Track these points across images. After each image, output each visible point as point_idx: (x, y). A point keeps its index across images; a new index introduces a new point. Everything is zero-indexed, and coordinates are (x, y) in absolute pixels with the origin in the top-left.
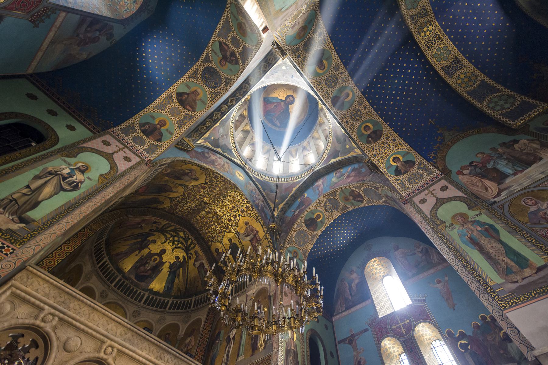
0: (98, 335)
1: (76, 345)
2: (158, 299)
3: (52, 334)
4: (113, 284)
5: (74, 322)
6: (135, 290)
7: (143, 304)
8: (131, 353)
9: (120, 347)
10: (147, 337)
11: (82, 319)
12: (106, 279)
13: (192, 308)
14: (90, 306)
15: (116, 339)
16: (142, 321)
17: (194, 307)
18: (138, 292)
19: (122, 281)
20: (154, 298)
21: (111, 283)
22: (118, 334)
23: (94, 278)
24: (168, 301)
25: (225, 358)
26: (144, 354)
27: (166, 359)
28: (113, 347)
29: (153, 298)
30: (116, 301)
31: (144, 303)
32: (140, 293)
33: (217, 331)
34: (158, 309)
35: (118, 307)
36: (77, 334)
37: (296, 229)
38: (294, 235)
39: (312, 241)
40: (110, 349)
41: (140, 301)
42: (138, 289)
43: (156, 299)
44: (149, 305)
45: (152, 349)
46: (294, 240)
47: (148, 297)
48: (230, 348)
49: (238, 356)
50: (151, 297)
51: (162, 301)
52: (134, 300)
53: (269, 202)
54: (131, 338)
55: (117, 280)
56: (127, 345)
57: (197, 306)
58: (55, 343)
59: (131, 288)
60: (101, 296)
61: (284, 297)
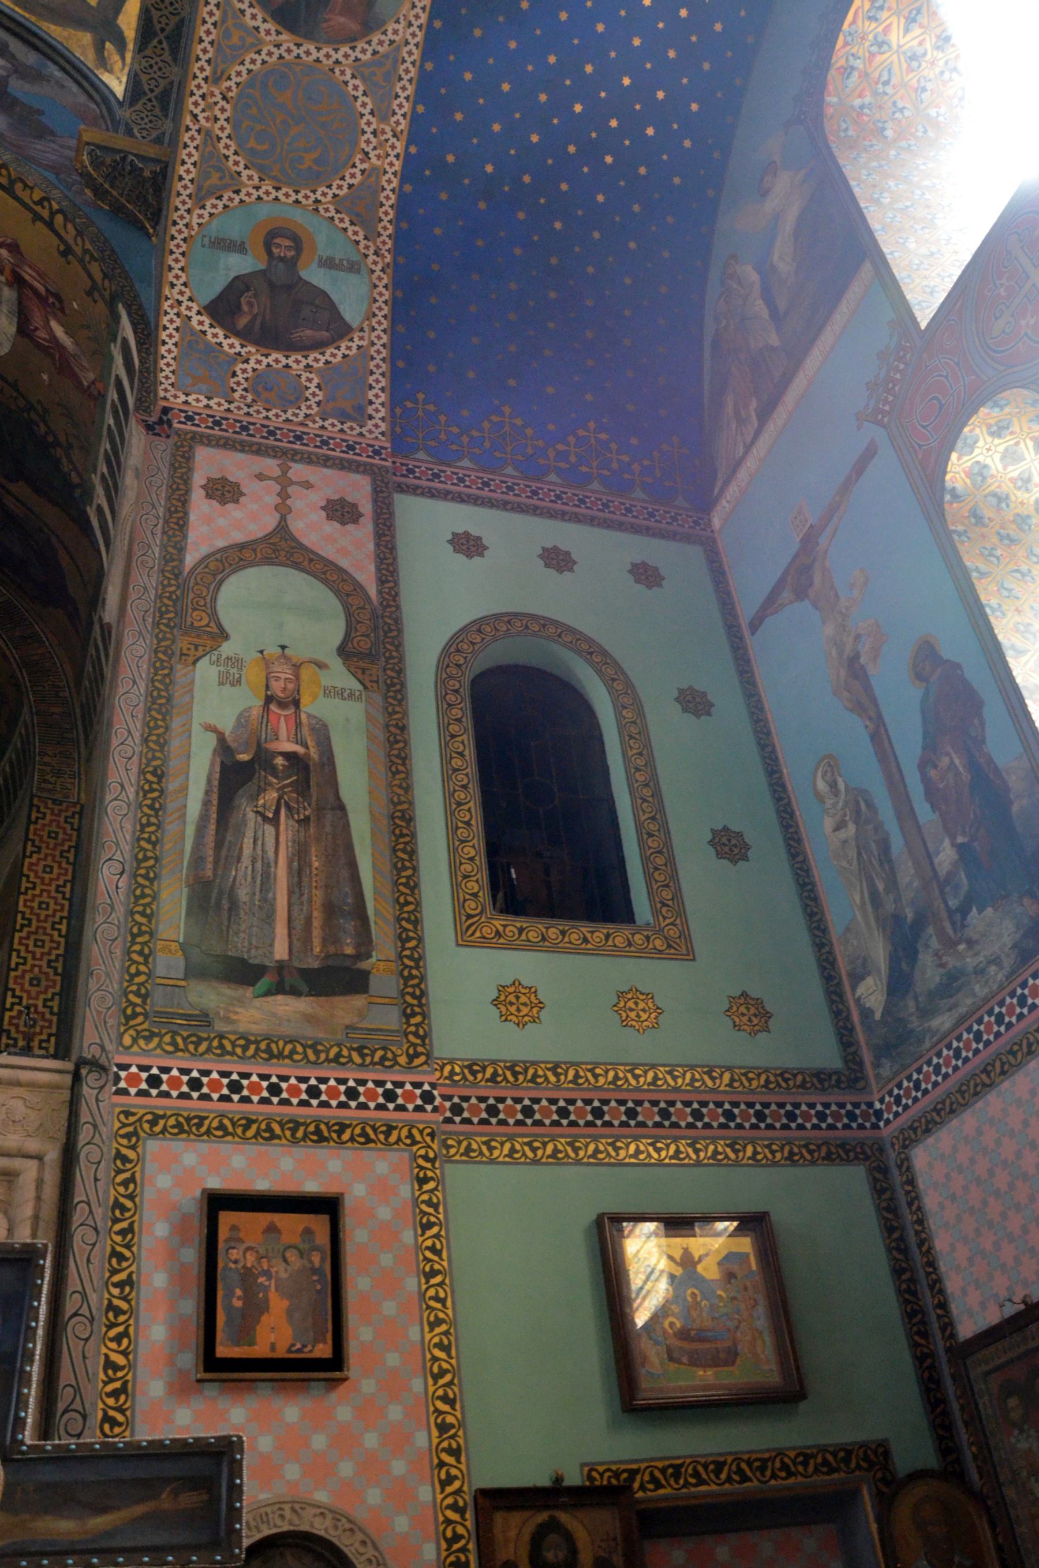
37: (216, 79)
38: (222, 129)
39: (382, 113)
46: (236, 163)
53: (56, 32)
61: (200, 505)
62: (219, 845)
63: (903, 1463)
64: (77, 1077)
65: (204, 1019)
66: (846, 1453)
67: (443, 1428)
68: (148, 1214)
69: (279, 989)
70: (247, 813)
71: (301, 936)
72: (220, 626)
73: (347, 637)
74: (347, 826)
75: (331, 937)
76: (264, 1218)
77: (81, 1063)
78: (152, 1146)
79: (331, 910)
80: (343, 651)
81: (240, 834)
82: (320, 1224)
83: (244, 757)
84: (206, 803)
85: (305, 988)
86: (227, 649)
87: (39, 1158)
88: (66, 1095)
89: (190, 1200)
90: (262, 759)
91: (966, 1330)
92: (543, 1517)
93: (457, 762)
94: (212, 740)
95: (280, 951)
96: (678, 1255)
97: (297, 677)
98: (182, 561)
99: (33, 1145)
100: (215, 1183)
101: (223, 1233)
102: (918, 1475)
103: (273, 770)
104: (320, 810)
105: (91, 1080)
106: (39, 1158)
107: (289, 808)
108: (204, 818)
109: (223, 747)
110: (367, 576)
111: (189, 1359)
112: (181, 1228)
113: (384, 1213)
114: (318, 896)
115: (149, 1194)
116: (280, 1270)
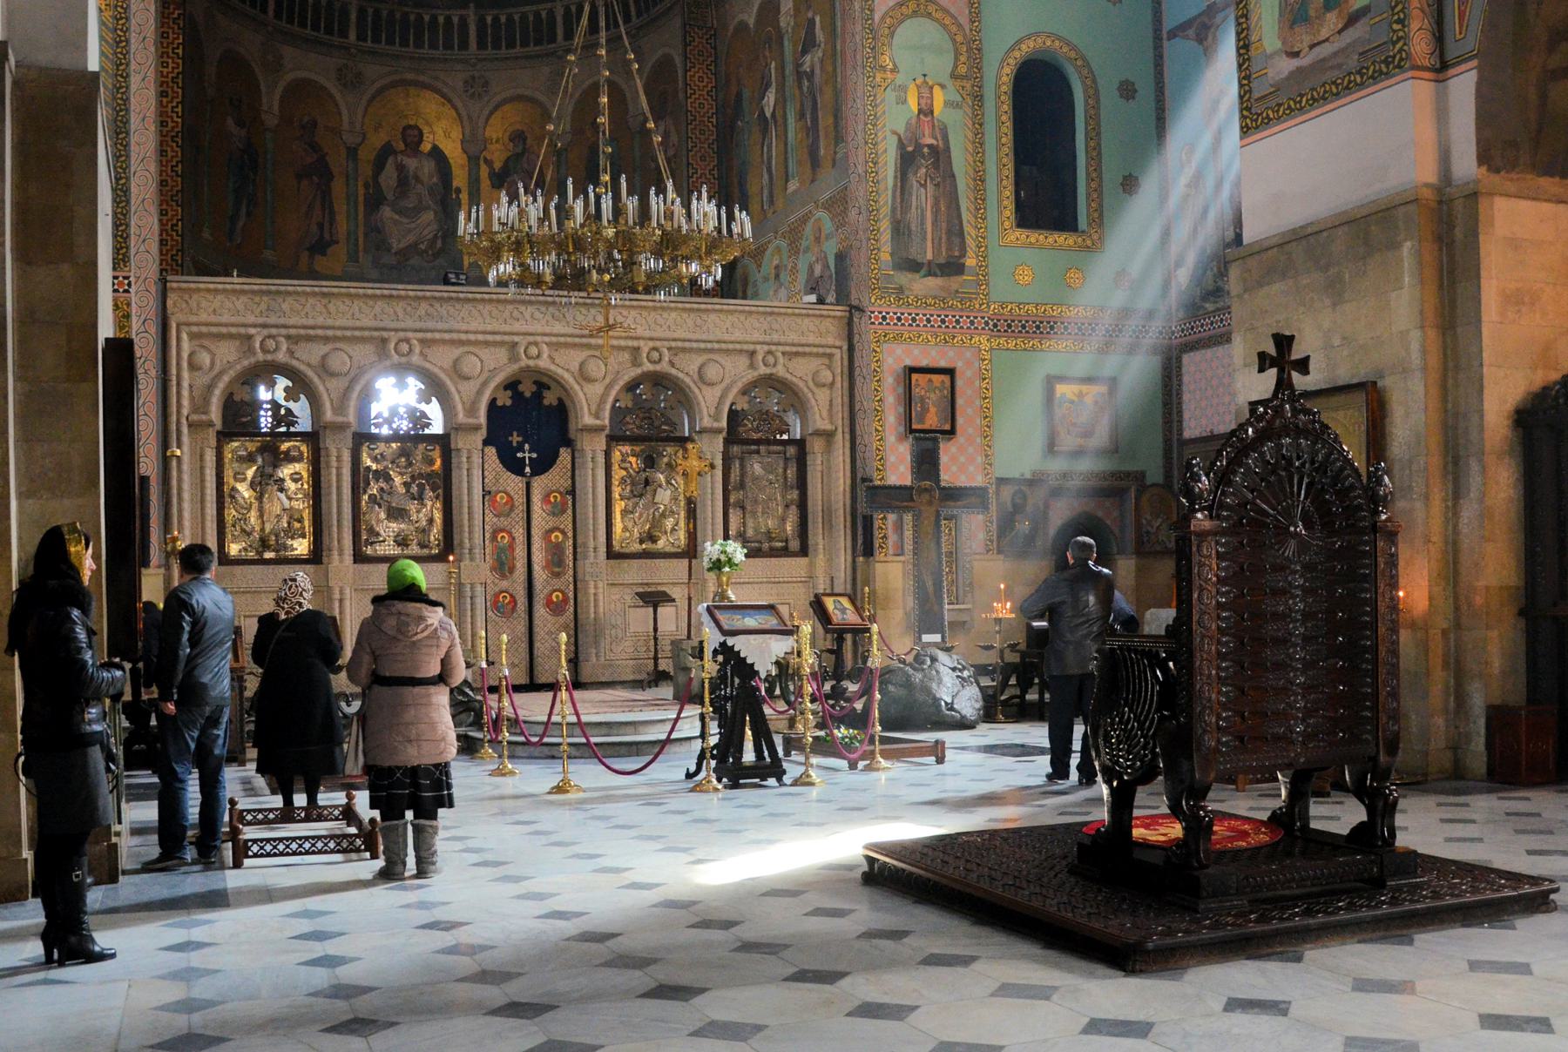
0: (366, 333)
1: (344, 363)
2: (516, 17)
3: (295, 363)
4: (352, 36)
5: (311, 332)
6: (427, 18)
7: (479, 49)
8: (447, 336)
9: (420, 335)
10: (461, 295)
11: (320, 320)
12: (322, 35)
13: (634, 19)
14: (314, 294)
15: (403, 325)
16: (505, 102)
17: (639, 14)
18: (441, 19)
19: (370, 11)
20: (503, 19)
21: (344, 33)
22: (401, 316)
23: (288, 52)
24: (551, 13)
25: (766, 176)
26: (473, 326)
27: (528, 316)
28: (407, 341)
29: (496, 19)
30: (397, 77)
31: (481, 44)
32: (448, 19)
33: (734, 90)
34: (532, 49)
35: (412, 90)
36: (329, 347)
40: (404, 347)
41: (464, 45)
42: (434, 11)
43: (510, 19)
44: (496, 46)
45: (485, 312)
47: (481, 22)
48: (770, 150)
49: (787, 181)
50: (489, 19)
51: (531, 18)
52: (445, 48)
54: (431, 310)
55: (353, 17)
56: (430, 324)
57: (647, 9)
58: (310, 373)
59: (412, 17)
60: (345, 85)
62: (902, 201)
63: (1149, 481)
64: (850, 312)
65: (900, 290)
66: (1128, 474)
67: (987, 456)
68: (886, 375)
69: (930, 274)
70: (913, 182)
71: (937, 249)
72: (895, 65)
73: (956, 66)
74: (955, 187)
75: (949, 249)
76: (929, 376)
77: (851, 307)
78: (885, 346)
79: (949, 232)
80: (954, 76)
81: (910, 195)
82: (946, 379)
83: (910, 149)
84: (896, 177)
85: (939, 273)
86: (900, 79)
87: (840, 348)
88: (846, 320)
89: (899, 367)
90: (918, 147)
91: (1187, 434)
92: (1017, 488)
93: (1004, 140)
94: (895, 138)
95: (929, 256)
96: (1076, 392)
97: (931, 93)
98: (873, 19)
99: (838, 343)
100: (908, 362)
101: (913, 382)
102: (1153, 485)
103: (923, 156)
104: (944, 178)
105: (856, 314)
106: (840, 348)
107: (932, 179)
108: (895, 186)
109: (901, 145)
110: (964, 20)
111: (902, 429)
112: (897, 381)
113: (969, 374)
114: (944, 225)
115: (885, 367)
116: (932, 396)
